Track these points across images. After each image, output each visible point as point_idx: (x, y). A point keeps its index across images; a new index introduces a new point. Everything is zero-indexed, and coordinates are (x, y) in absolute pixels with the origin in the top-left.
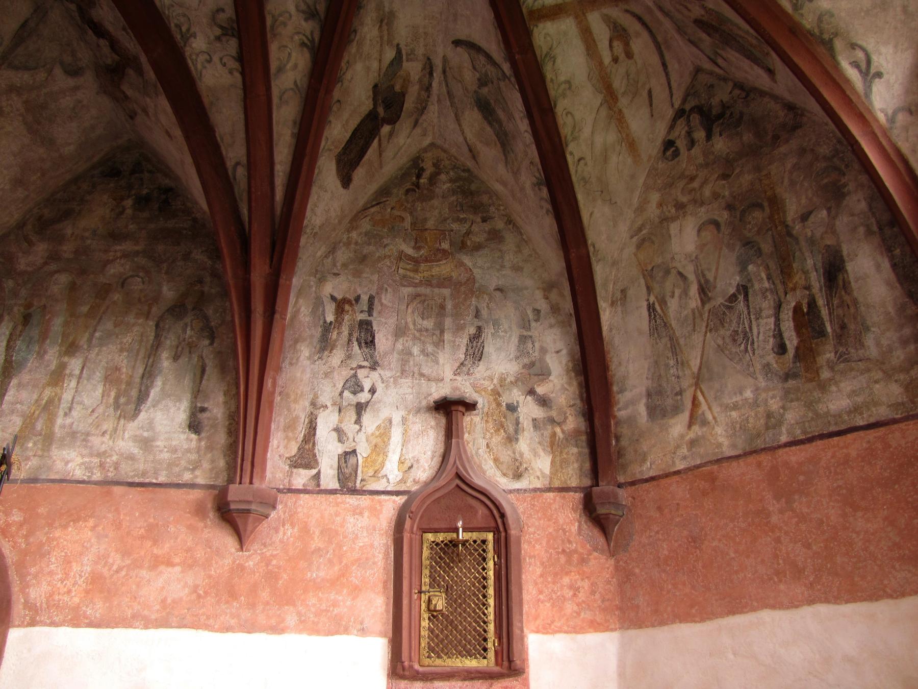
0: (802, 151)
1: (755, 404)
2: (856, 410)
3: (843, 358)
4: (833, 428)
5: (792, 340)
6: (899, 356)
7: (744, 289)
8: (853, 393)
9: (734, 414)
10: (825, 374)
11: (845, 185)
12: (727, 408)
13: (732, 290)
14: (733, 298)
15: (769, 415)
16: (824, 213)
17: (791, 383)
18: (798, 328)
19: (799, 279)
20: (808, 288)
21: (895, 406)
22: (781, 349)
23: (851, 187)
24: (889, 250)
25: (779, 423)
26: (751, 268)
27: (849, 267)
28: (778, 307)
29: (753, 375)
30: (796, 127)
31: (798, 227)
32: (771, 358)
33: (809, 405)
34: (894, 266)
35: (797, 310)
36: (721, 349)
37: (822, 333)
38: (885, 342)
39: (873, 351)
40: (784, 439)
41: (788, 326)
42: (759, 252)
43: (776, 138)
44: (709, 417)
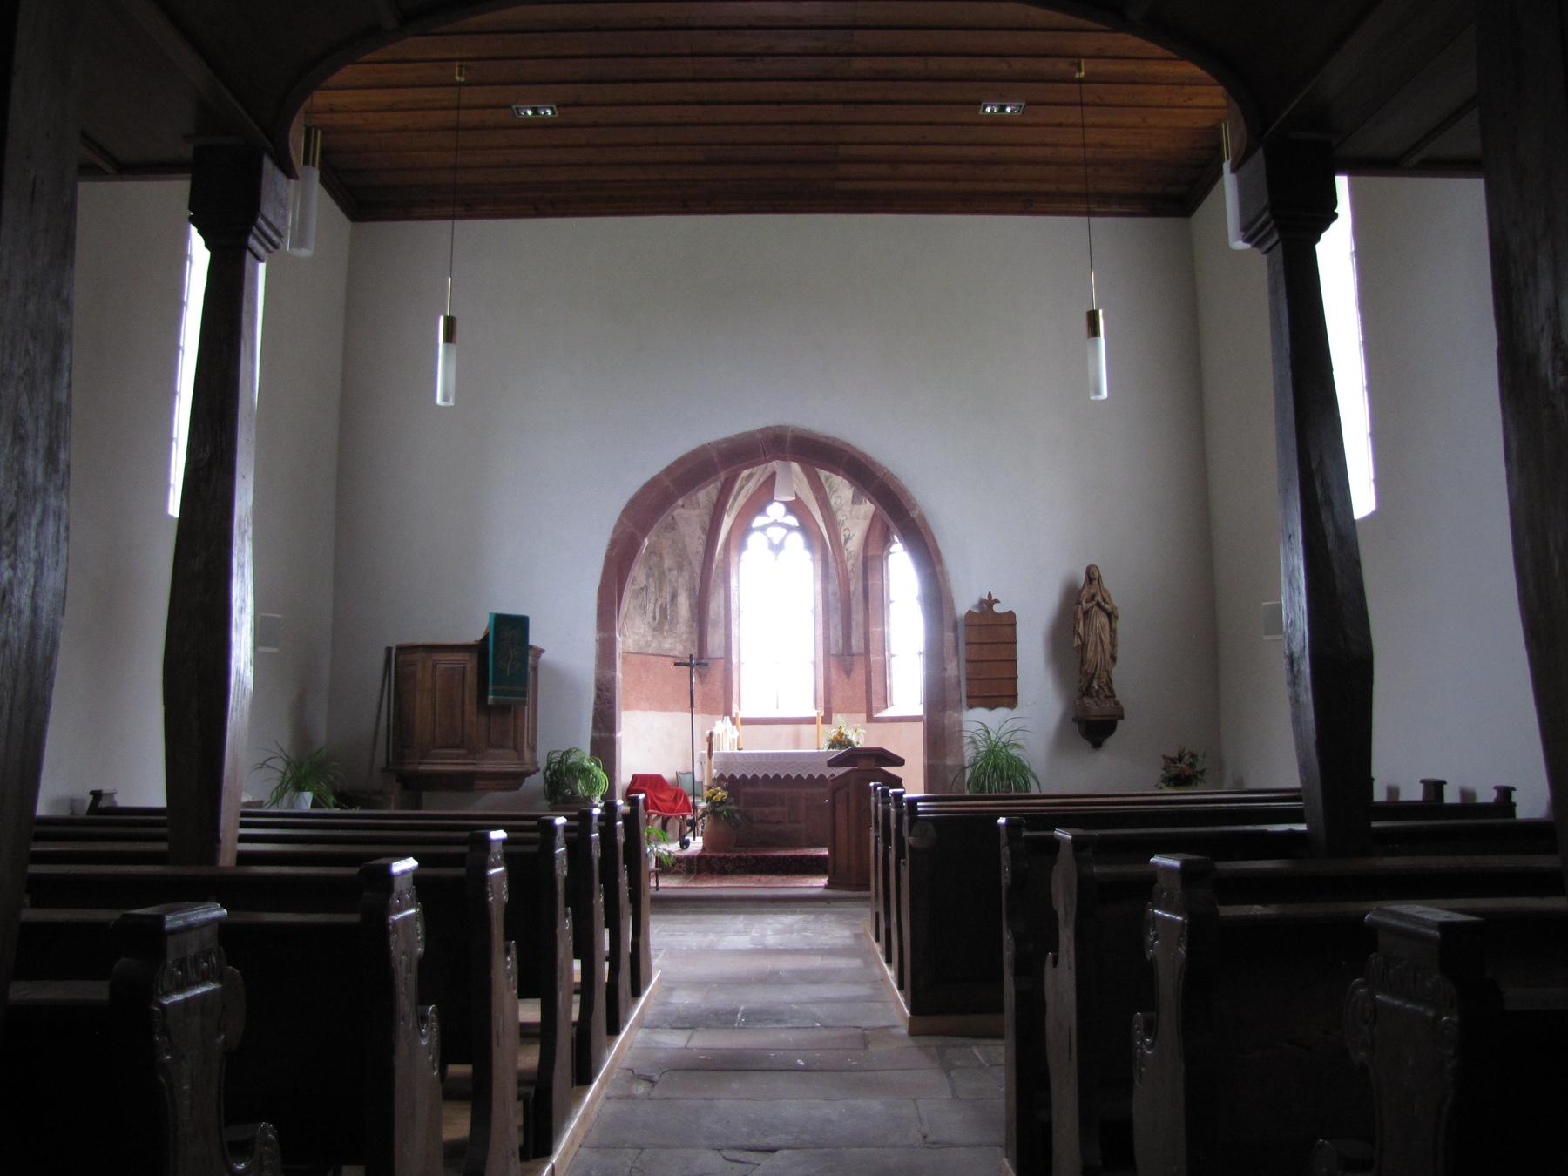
0: (674, 542)
1: (643, 636)
2: (671, 650)
3: (670, 630)
4: (664, 654)
5: (658, 617)
6: (684, 637)
7: (646, 588)
8: (671, 644)
9: (636, 637)
10: (665, 634)
11: (684, 566)
12: (634, 633)
13: (643, 586)
14: (642, 589)
15: (647, 642)
16: (676, 573)
17: (655, 633)
18: (661, 612)
19: (664, 594)
20: (666, 599)
21: (680, 652)
22: (654, 618)
23: (685, 568)
24: (690, 599)
25: (650, 646)
26: (651, 580)
27: (679, 598)
28: (656, 600)
29: (645, 625)
30: (673, 528)
31: (667, 573)
32: (651, 620)
33: (660, 643)
34: (690, 605)
35: (661, 605)
36: (635, 608)
37: (666, 618)
38: (682, 630)
39: (678, 632)
40: (650, 652)
41: (658, 610)
42: (654, 575)
43: (666, 528)
44: (627, 634)
